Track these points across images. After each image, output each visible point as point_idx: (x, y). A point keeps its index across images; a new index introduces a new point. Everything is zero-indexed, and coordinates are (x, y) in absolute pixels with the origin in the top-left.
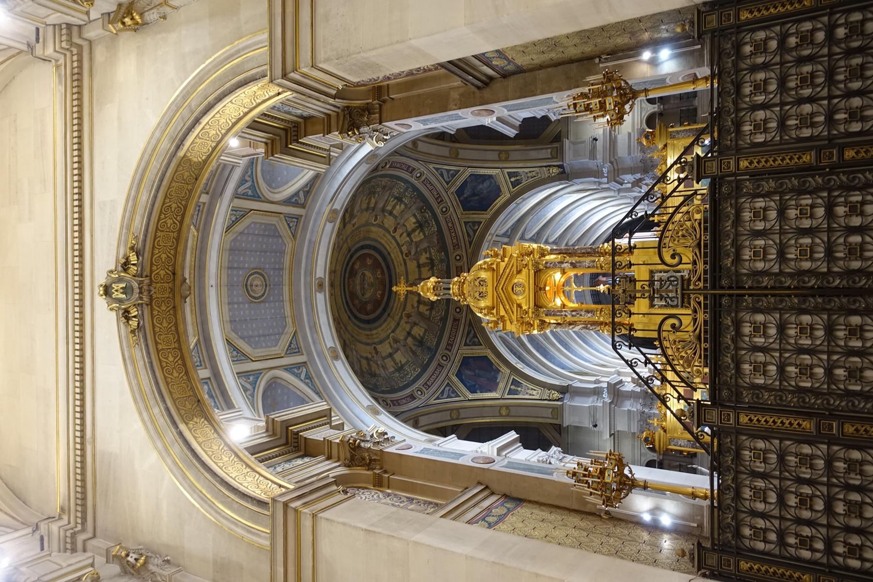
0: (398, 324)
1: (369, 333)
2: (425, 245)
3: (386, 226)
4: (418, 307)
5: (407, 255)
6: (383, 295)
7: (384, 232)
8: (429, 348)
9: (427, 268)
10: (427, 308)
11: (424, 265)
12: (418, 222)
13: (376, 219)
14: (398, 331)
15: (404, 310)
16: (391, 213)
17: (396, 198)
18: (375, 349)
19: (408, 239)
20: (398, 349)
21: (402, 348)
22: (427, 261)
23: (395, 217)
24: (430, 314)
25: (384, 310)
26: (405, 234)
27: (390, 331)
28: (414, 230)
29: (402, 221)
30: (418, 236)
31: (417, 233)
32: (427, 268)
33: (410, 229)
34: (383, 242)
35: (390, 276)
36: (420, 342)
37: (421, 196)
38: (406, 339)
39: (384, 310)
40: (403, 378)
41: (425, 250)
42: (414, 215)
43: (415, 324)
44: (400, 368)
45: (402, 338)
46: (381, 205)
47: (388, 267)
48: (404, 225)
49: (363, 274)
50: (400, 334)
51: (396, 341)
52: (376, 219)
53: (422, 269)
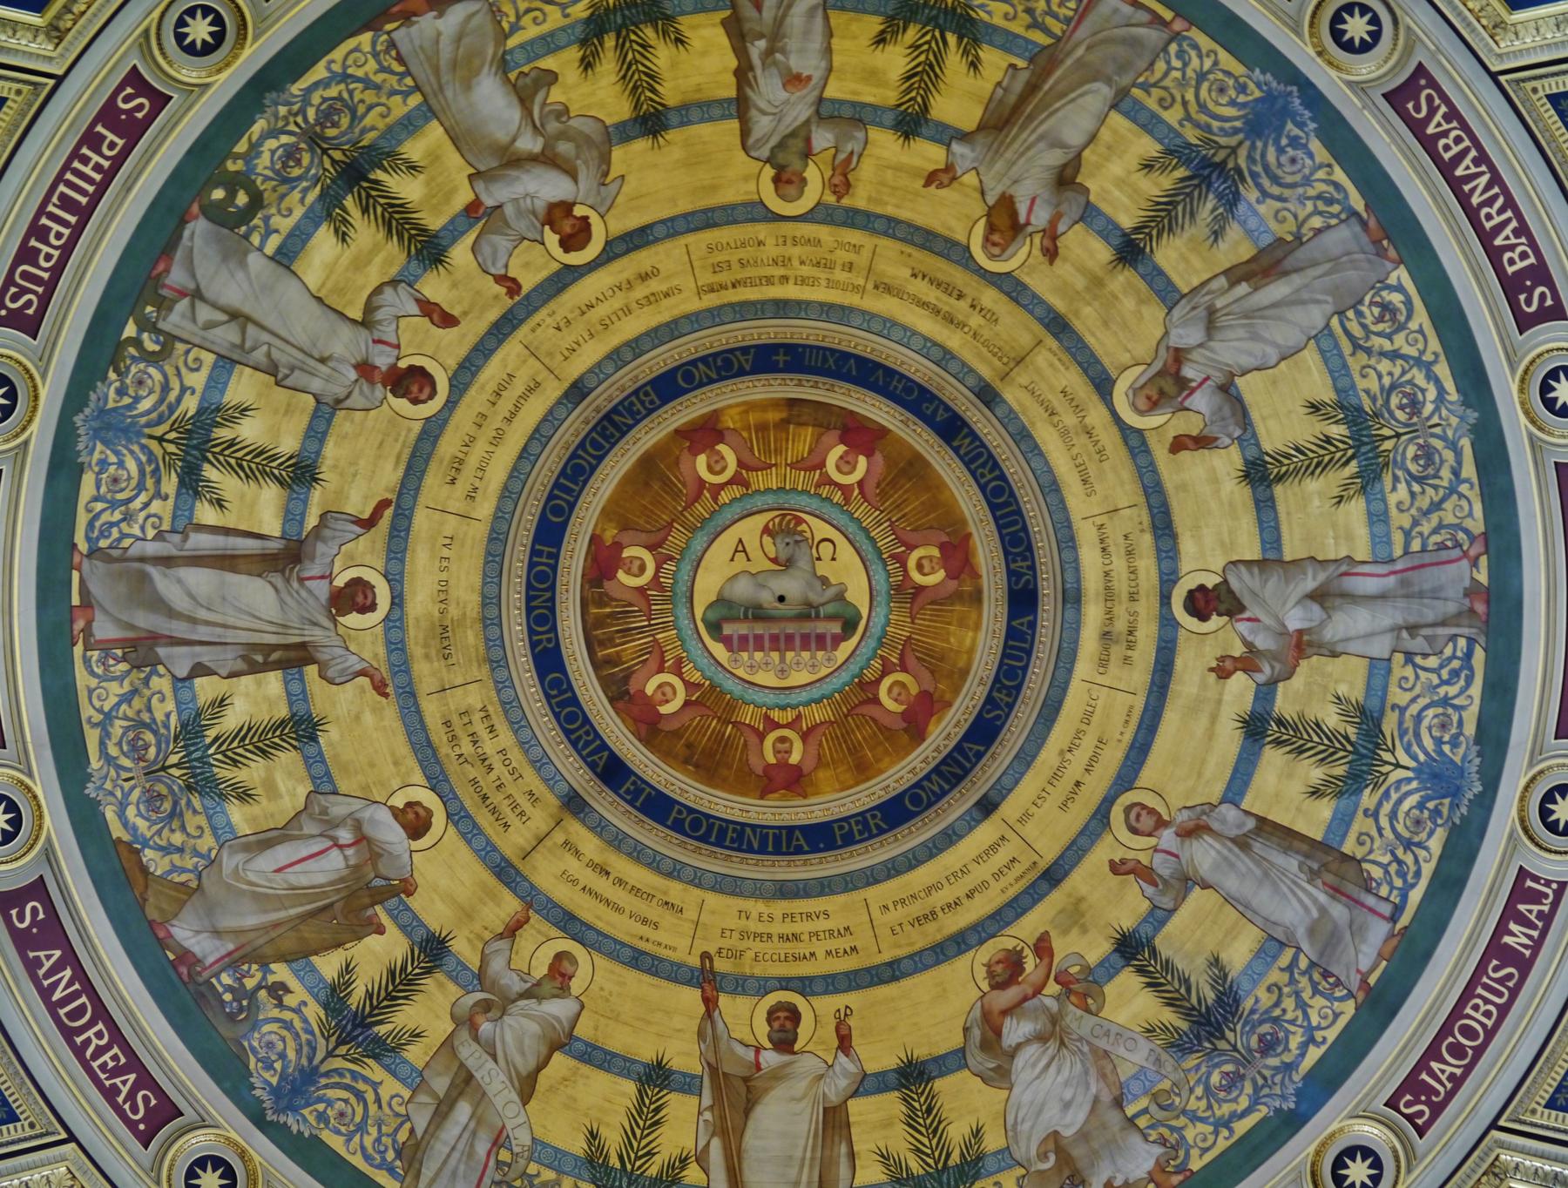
0: (1058, 325)
1: (1093, 615)
2: (491, 102)
3: (389, 477)
4: (948, 135)
5: (576, 237)
6: (859, 435)
7: (433, 482)
8: (1263, 121)
9: (663, 56)
10: (954, 61)
11: (639, 80)
12: (328, 210)
13: (354, 597)
14: (1104, 344)
15: (955, 251)
16: (300, 474)
17: (192, 483)
18: (1202, 603)
19: (460, 254)
20: (1227, 389)
21: (1231, 350)
22: (608, 65)
23: (325, 412)
24: (1008, 42)
25: (951, 428)
26: (434, 287)
27: (1097, 415)
28: (397, 219)
29: (346, 344)
30: (430, 180)
31: (406, 188)
32: (663, 56)
33: (390, 256)
34: (498, 474)
35: (725, 365)
36: (1206, 174)
37: (140, 282)
38: (1166, 293)
39: (951, 428)
40: (1427, 454)
41: (528, 89)
42: (286, 258)
43: (1066, 179)
44: (1360, 443)
45: (1154, 314)
46: (257, 602)
47: (668, 387)
48: (366, 323)
49: (724, 613)
50: (1129, 330)
51: (1168, 384)
52: (354, 597)
53: (670, 93)
